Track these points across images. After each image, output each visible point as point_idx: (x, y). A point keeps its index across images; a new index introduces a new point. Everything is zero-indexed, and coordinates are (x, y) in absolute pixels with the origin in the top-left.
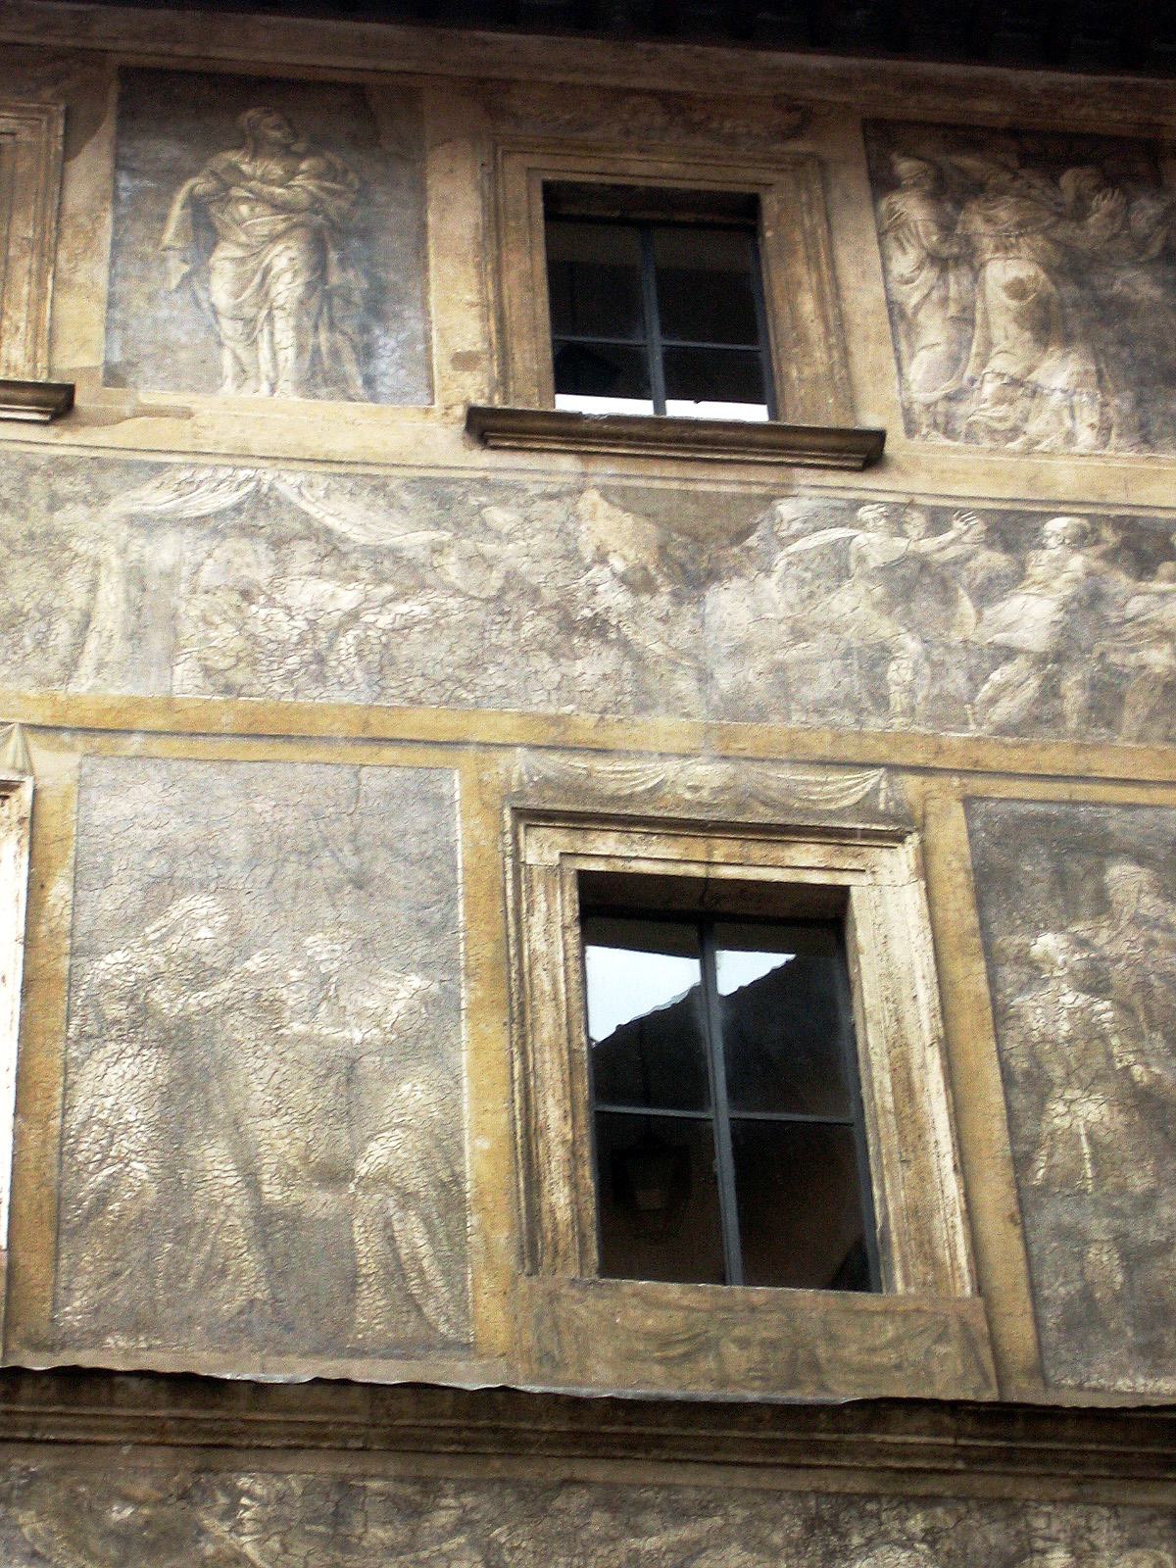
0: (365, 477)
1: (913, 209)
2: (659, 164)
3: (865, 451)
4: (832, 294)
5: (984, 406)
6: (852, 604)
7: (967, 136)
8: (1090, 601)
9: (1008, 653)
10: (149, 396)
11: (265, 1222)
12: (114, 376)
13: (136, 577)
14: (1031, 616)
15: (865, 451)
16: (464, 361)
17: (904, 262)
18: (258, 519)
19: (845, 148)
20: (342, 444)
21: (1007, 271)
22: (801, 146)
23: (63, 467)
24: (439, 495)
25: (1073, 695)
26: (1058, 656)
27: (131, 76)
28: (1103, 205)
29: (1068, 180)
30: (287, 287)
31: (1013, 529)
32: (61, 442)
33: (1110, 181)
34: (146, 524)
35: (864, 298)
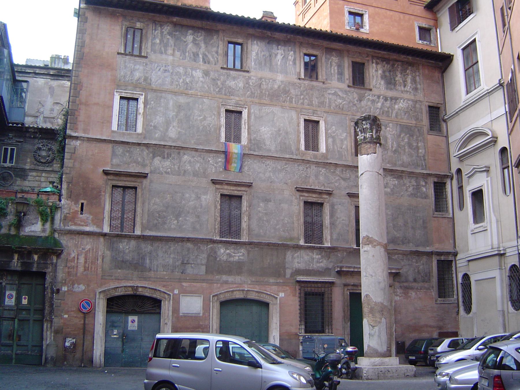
0: (341, 90)
1: (374, 65)
2: (358, 60)
3: (371, 90)
4: (369, 75)
5: (378, 86)
6: (369, 103)
7: (378, 58)
8: (383, 104)
9: (378, 108)
10: (329, 82)
11: (338, 151)
12: (326, 79)
13: (329, 98)
14: (379, 105)
15: (371, 90)
16: (347, 79)
17: (374, 71)
18: (335, 94)
19: (370, 58)
20: (340, 87)
21: (380, 72)
22: (367, 58)
23: (324, 88)
24: (346, 92)
25: (381, 112)
26: (381, 109)
27: (326, 48)
28: (386, 66)
29: (384, 63)
30: (336, 71)
31: (379, 97)
32: (324, 86)
33: (386, 63)
34: (329, 94)
35: (371, 75)
